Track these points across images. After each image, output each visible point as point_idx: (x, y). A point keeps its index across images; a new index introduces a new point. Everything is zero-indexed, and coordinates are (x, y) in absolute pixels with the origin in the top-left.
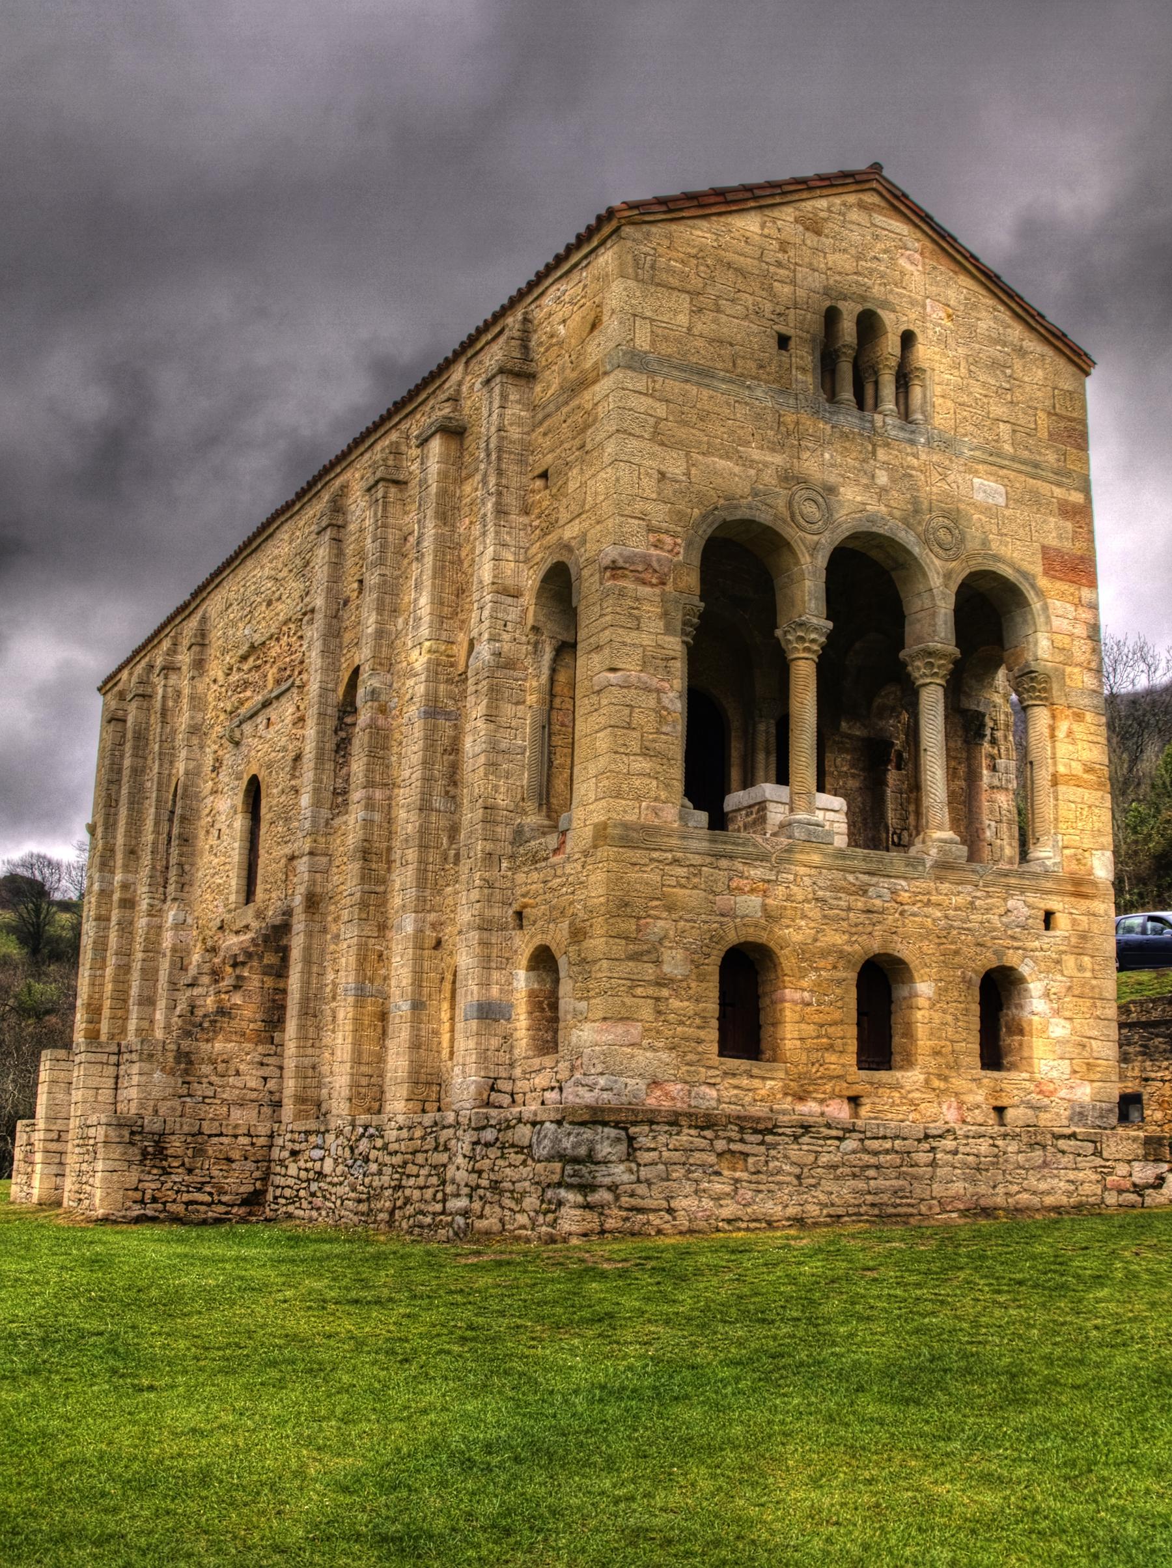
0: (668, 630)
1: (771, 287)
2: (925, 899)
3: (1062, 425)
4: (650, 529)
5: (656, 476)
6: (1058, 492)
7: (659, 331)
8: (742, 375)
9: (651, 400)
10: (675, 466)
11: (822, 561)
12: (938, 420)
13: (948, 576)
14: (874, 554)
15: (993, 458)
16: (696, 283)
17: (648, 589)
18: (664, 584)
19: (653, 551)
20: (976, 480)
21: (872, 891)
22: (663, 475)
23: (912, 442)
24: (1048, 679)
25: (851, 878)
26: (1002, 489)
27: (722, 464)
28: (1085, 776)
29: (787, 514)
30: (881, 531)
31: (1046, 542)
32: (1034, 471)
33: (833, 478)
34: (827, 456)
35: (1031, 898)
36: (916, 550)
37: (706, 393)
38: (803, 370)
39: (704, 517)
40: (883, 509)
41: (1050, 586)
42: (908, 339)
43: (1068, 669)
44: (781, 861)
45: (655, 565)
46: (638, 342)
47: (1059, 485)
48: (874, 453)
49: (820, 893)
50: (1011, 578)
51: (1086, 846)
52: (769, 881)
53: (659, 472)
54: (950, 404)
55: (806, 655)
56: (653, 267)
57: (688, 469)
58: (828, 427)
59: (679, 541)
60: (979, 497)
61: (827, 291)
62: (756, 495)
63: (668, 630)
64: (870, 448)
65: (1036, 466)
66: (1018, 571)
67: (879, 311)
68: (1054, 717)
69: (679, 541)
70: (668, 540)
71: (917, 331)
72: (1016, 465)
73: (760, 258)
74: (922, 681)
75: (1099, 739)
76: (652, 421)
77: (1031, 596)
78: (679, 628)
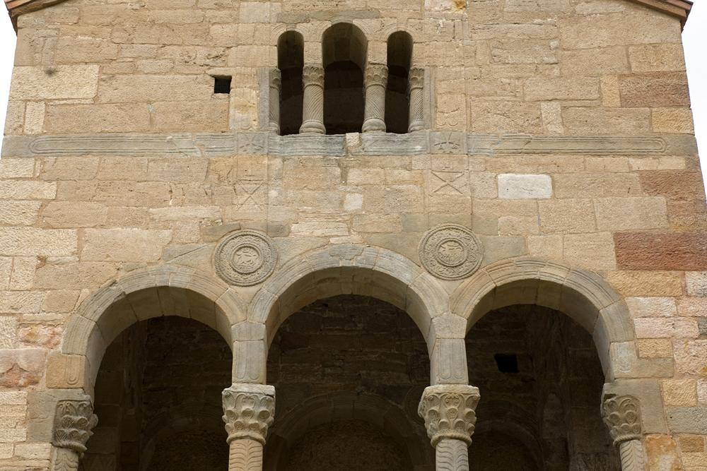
0: (33, 437)
1: (207, 32)
3: (644, 84)
4: (21, 324)
5: (36, 262)
6: (639, 164)
7: (56, 110)
8: (162, 131)
9: (37, 182)
10: (60, 245)
11: (261, 315)
12: (440, 121)
13: (455, 300)
15: (531, 148)
16: (111, 50)
17: (13, 393)
18: (36, 383)
19: (22, 348)
20: (503, 177)
22: (43, 260)
23: (403, 153)
24: (632, 402)
26: (546, 179)
27: (122, 233)
29: (211, 270)
31: (622, 228)
32: (599, 146)
33: (279, 216)
34: (273, 193)
36: (405, 277)
37: (110, 160)
38: (244, 107)
39: (96, 296)
40: (355, 237)
41: (629, 280)
42: (400, 46)
43: (667, 384)
45: (23, 363)
46: (27, 126)
47: (641, 155)
48: (344, 176)
50: (565, 283)
53: (39, 258)
54: (460, 98)
55: (239, 433)
56: (54, 48)
57: (80, 248)
58: (277, 162)
59: (59, 329)
60: (504, 195)
61: (281, 19)
62: (170, 257)
63: (33, 437)
64: (338, 171)
65: (602, 140)
66: (576, 272)
67: (356, 22)
68: (649, 451)
69: (59, 329)
70: (44, 332)
71: (409, 30)
72: (570, 146)
73: (195, 7)
74: (436, 436)
76: (36, 205)
77: (596, 297)
78: (49, 429)
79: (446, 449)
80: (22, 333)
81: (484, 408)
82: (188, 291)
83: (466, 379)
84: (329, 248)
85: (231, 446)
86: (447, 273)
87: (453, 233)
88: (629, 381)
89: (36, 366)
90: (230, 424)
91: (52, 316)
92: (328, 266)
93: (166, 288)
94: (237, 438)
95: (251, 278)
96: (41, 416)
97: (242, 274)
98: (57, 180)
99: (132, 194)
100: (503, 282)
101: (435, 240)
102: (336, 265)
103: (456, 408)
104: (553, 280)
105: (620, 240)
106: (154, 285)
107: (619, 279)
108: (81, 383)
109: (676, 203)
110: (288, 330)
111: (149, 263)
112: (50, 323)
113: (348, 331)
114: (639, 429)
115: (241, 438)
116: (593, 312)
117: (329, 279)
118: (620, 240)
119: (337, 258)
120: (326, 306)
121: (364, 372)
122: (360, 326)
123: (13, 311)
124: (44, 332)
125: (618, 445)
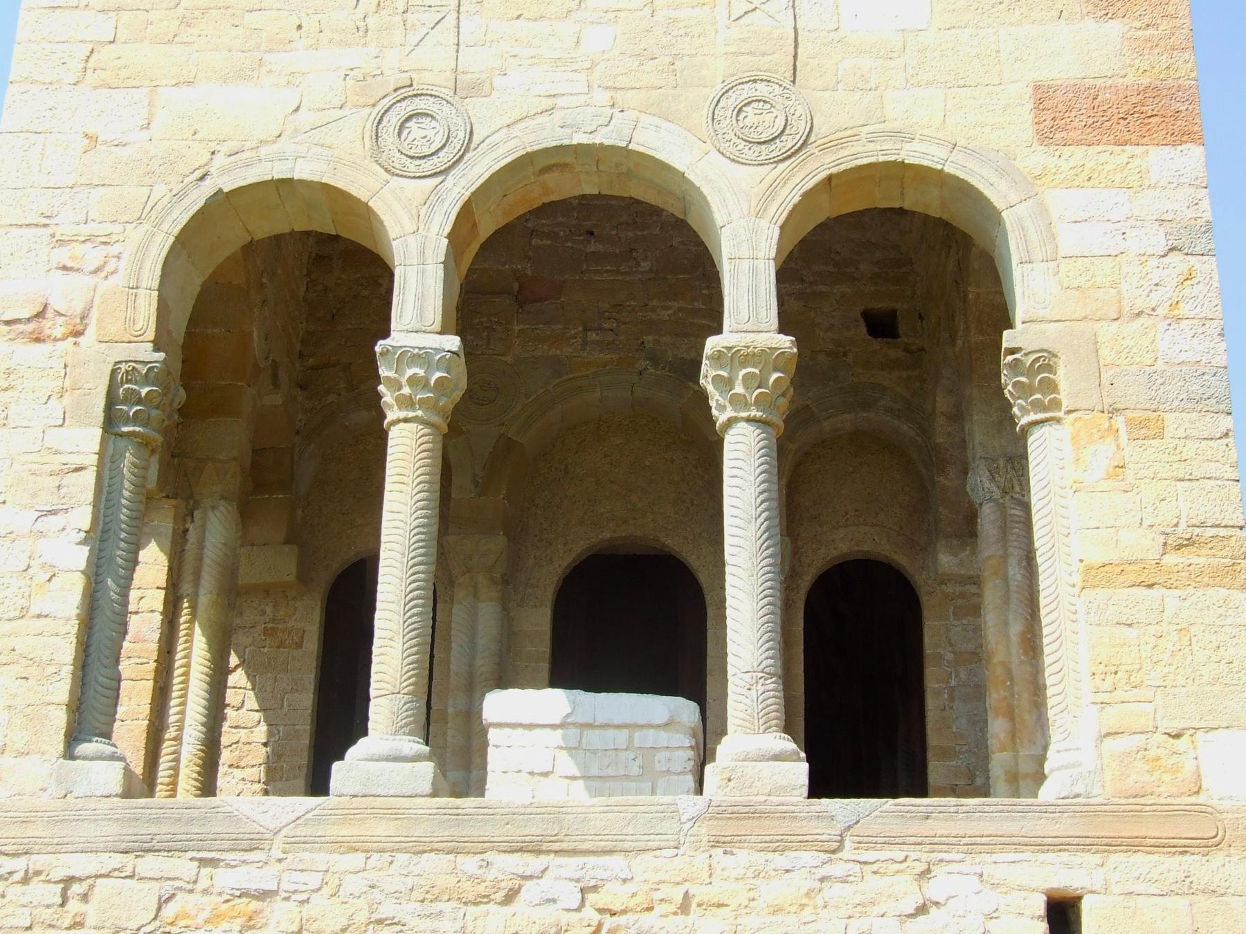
2: (677, 895)
14: (564, 187)
21: (530, 891)
22: (92, 139)
25: (469, 864)
28: (1171, 559)
30: (598, 140)
35: (1001, 866)
39: (179, 196)
44: (296, 843)
45: (57, 304)
49: (386, 910)
51: (1174, 726)
52: (264, 895)
55: (403, 414)
75: (1212, 469)
79: (740, 438)
80: (62, 255)
81: (808, 371)
82: (326, 187)
83: (774, 323)
84: (558, 116)
85: (391, 434)
86: (750, 154)
87: (762, 90)
88: (1044, 326)
89: (79, 308)
90: (388, 397)
91: (108, 228)
92: (554, 144)
93: (288, 182)
94: (399, 421)
95: (428, 166)
96: (86, 386)
97: (412, 158)
98: (118, 9)
99: (240, 30)
100: (843, 167)
101: (733, 100)
102: (566, 142)
103: (757, 371)
104: (926, 163)
105: (1042, 96)
106: (269, 178)
107: (1035, 159)
108: (151, 334)
109: (1140, 33)
110: (529, 272)
111: (263, 142)
112: (104, 239)
113: (627, 273)
114: (1056, 404)
115: (406, 420)
116: (991, 215)
117: (556, 165)
118: (1042, 96)
119: (569, 131)
120: (592, 234)
121: (650, 338)
122: (645, 266)
123: (46, 221)
124: (94, 257)
125: (1025, 431)
